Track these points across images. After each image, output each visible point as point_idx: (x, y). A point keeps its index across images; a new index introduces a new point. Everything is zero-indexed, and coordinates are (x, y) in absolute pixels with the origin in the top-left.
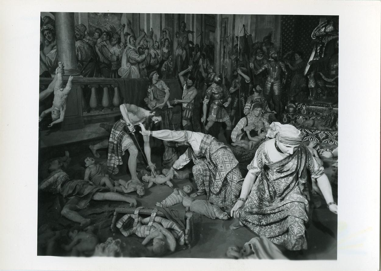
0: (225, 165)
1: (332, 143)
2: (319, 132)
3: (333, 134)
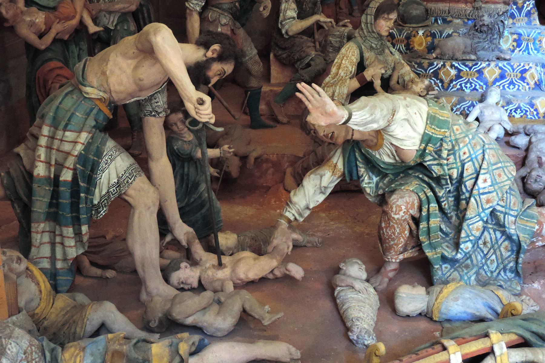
0: (508, 177)
1: (513, 89)
2: (484, 65)
3: (515, 67)
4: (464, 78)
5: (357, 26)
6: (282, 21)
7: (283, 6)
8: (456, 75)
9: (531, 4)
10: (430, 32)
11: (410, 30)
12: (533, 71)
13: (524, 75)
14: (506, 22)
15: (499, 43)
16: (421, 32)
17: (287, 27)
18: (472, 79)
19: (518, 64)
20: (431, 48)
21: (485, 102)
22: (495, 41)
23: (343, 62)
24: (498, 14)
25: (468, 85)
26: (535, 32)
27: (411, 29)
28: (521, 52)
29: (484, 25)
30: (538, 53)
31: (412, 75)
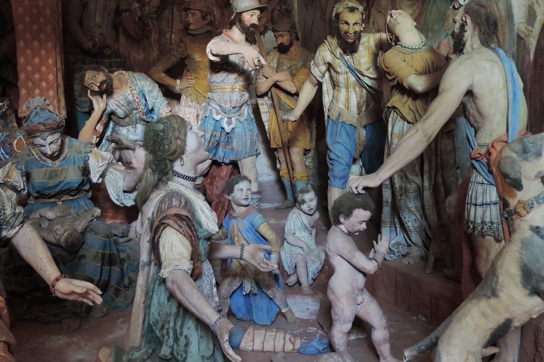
9: (6, 105)
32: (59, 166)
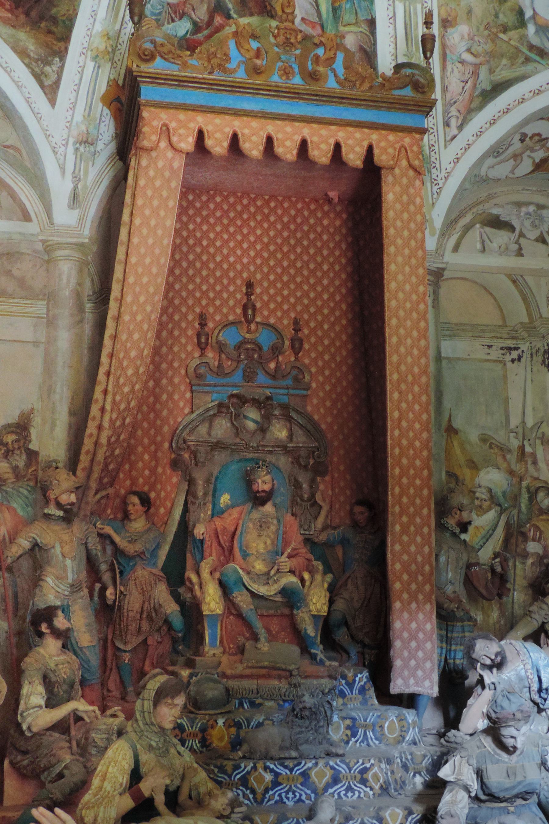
1: (352, 797)
2: (309, 765)
3: (351, 765)
4: (284, 785)
5: (130, 715)
6: (23, 712)
7: (25, 690)
8: (272, 781)
10: (234, 720)
11: (205, 719)
12: (376, 769)
13: (365, 776)
14: (334, 703)
15: (327, 732)
16: (221, 722)
17: (29, 720)
18: (295, 786)
19: (355, 761)
20: (236, 744)
21: (315, 819)
22: (321, 730)
23: (110, 770)
24: (323, 692)
25: (291, 795)
26: (373, 715)
27: (207, 717)
28: (358, 744)
29: (305, 708)
30: (380, 743)
31: (210, 785)
32: (517, 762)
